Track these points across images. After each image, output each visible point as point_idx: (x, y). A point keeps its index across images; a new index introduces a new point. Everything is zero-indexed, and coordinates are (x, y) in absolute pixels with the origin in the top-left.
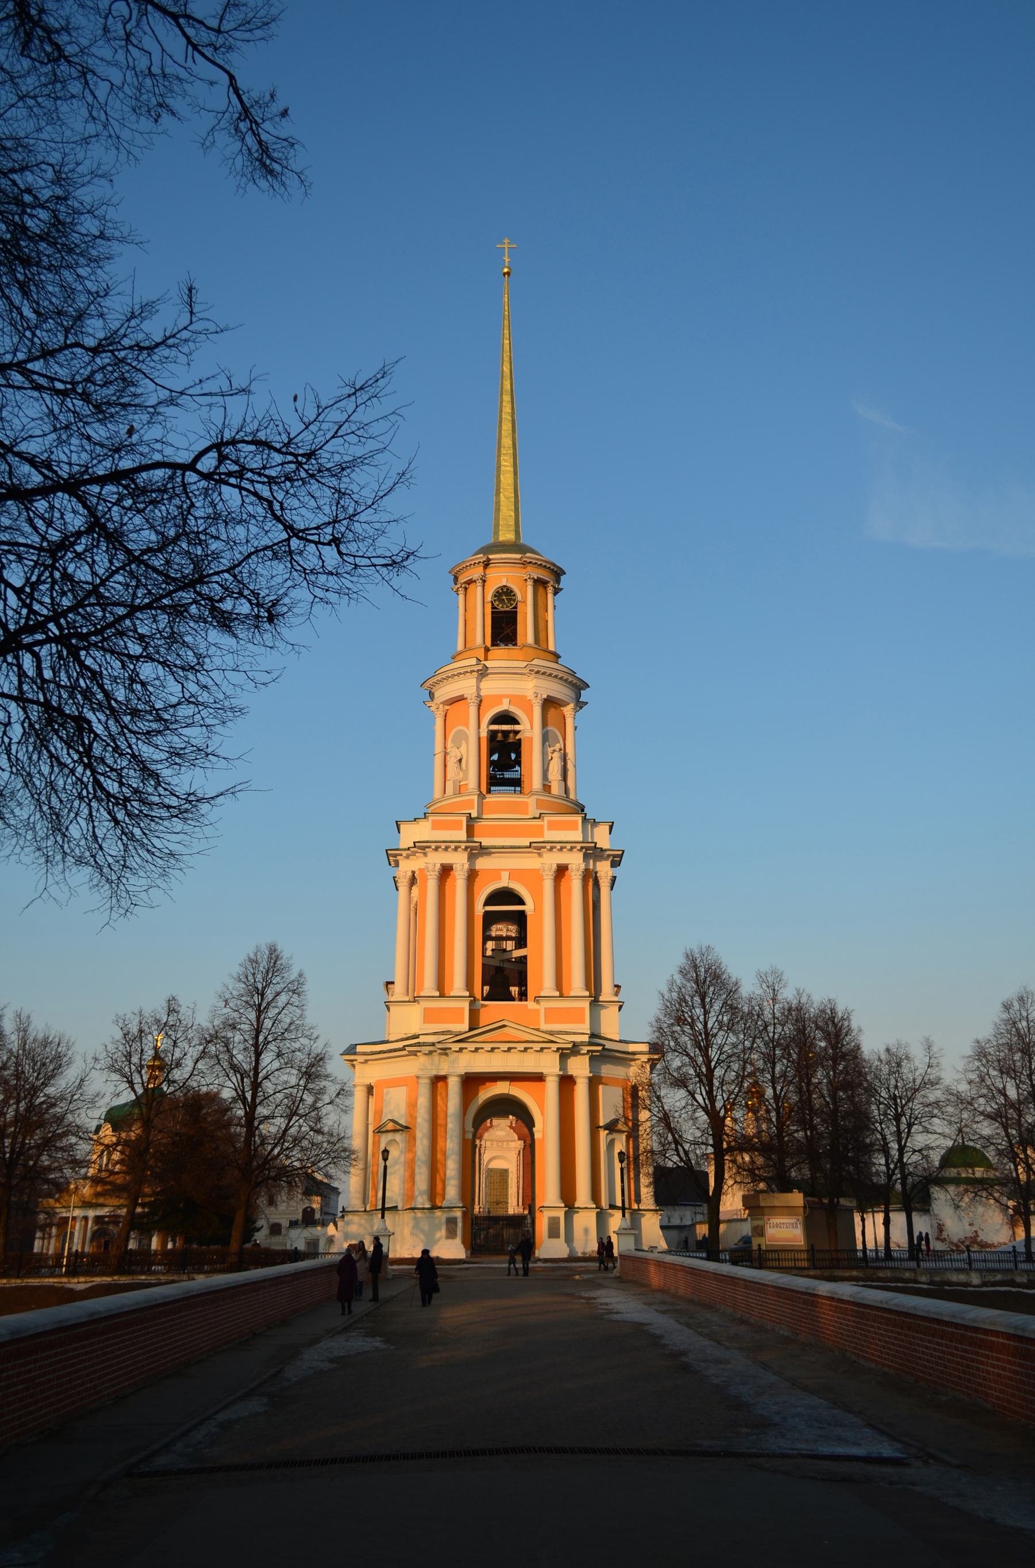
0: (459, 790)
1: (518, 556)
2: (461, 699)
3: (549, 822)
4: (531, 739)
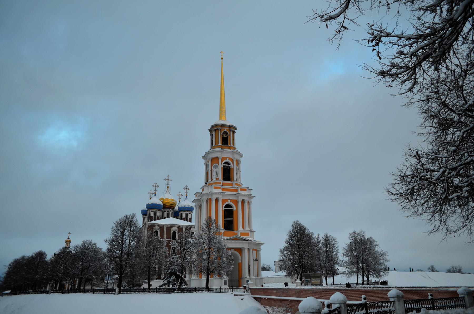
0: (217, 179)
2: (217, 158)
3: (240, 189)
4: (233, 168)
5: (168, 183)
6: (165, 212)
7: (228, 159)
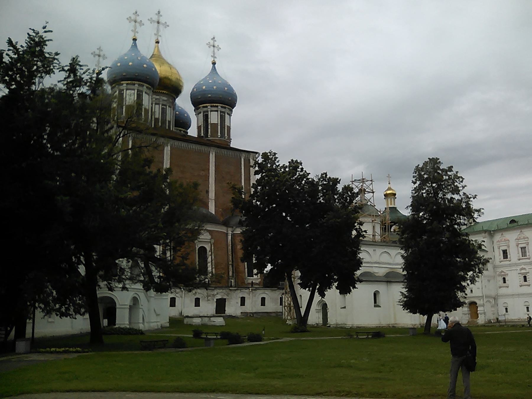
5: (158, 30)
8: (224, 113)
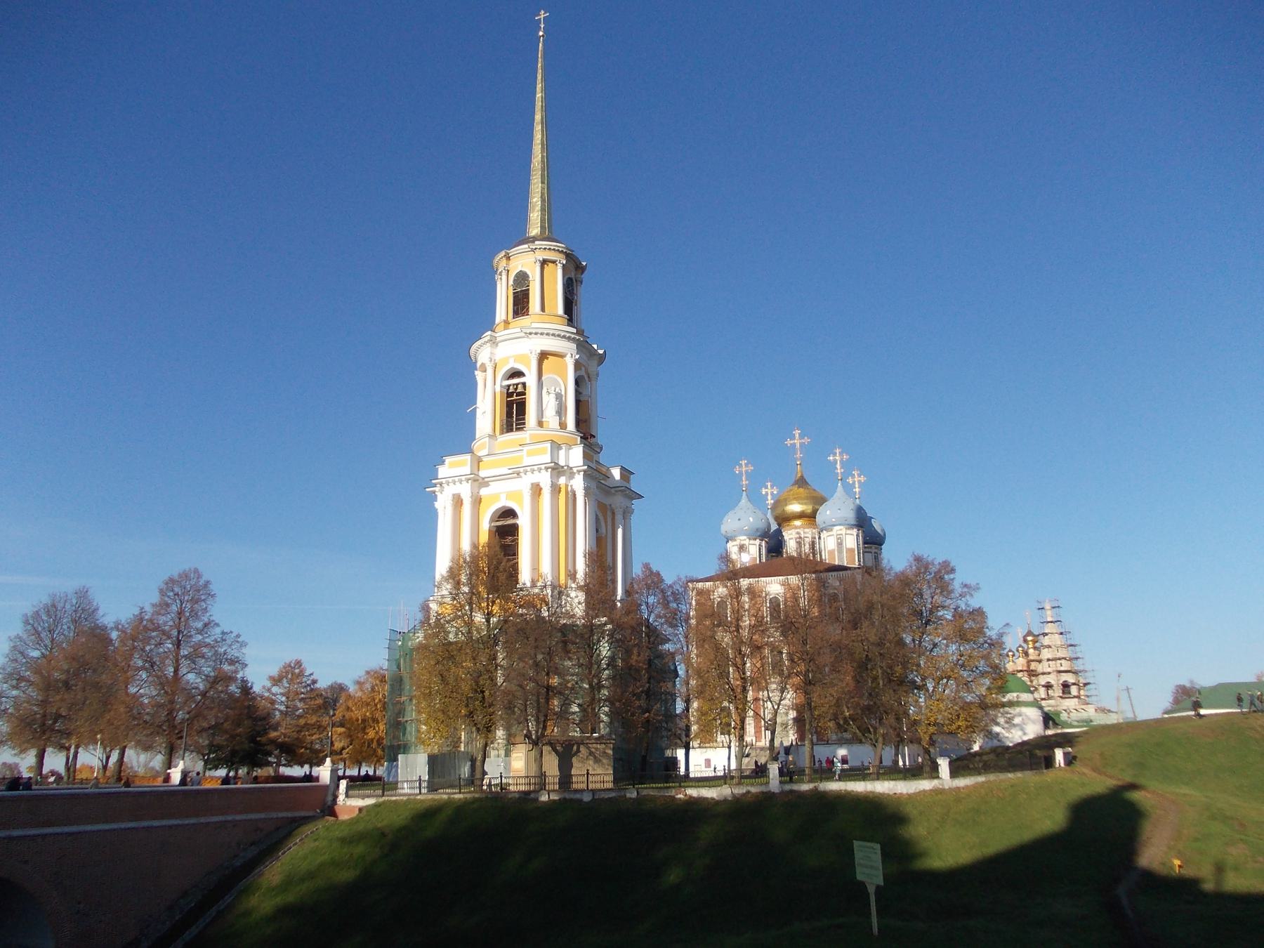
1: (526, 246)
6: (790, 539)
7: (511, 361)
8: (842, 535)
